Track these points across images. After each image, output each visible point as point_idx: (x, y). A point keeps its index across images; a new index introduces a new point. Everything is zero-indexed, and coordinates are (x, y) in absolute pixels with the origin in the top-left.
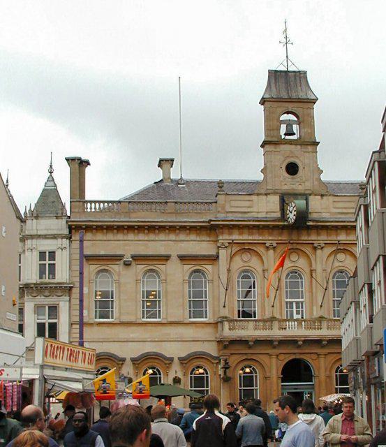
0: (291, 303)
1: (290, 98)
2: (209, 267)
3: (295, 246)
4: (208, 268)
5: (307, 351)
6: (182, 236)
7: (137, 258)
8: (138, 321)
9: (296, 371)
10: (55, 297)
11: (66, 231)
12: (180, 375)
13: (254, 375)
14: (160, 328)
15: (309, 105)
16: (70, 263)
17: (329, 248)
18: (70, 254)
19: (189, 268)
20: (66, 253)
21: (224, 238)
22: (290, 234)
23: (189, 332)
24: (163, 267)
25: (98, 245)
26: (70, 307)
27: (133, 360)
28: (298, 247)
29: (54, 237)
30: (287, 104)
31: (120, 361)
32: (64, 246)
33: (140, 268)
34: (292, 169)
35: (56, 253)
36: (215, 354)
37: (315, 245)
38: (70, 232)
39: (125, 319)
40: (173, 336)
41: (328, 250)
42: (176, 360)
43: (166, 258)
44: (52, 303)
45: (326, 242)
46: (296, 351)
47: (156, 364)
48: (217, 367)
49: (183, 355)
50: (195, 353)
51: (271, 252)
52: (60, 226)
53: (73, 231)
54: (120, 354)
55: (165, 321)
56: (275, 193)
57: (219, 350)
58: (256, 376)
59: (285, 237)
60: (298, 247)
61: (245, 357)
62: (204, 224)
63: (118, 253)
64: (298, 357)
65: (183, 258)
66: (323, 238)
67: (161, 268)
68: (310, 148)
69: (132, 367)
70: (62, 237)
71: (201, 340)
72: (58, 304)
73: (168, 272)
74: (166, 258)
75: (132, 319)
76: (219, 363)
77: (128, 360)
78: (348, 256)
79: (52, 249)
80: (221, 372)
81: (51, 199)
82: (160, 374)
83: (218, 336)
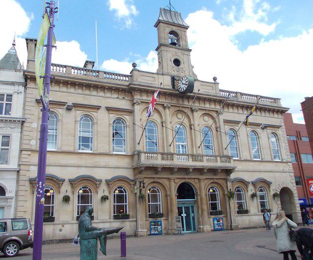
0: (179, 146)
1: (174, 23)
2: (127, 117)
3: (181, 109)
4: (127, 118)
5: (192, 177)
6: (108, 94)
7: (76, 106)
8: (76, 151)
9: (186, 191)
10: (9, 129)
11: (23, 81)
12: (69, 194)
13: (216, 193)
14: (92, 157)
15: (185, 29)
16: (24, 105)
17: (200, 112)
18: (25, 98)
19: (113, 116)
20: (22, 96)
21: (137, 97)
22: (178, 101)
23: (113, 161)
24: (95, 114)
25: (57, 94)
26: (21, 138)
27: (106, 181)
28: (183, 109)
29: (13, 84)
30: (173, 27)
31: (60, 181)
32: (20, 91)
33: (78, 113)
34: (177, 62)
35: (13, 96)
36: (131, 178)
37: (193, 109)
38: (26, 81)
39: (65, 149)
40: (102, 164)
41: (200, 113)
42: (104, 181)
43: (98, 108)
44: (5, 133)
45: (142, 101)
46: (186, 177)
47: (88, 185)
48: (134, 188)
49: (109, 178)
50: (117, 177)
51: (167, 110)
52: (18, 77)
53: (28, 81)
54: (97, 177)
55: (96, 152)
56: (168, 75)
57: (135, 175)
58: (159, 195)
59: (174, 102)
60: (183, 109)
61: (153, 180)
62: (124, 87)
63: (260, 123)
64: (187, 181)
65: (109, 109)
66: (197, 105)
67: (94, 114)
68: (186, 53)
69: (70, 187)
70: (19, 84)
71: (120, 167)
72: (11, 135)
73: (98, 118)
74: (98, 108)
75: (71, 149)
76: (135, 184)
77: (67, 181)
78: (210, 118)
79: (10, 92)
80: (137, 191)
81: (12, 60)
82: (91, 193)
83: (134, 164)
